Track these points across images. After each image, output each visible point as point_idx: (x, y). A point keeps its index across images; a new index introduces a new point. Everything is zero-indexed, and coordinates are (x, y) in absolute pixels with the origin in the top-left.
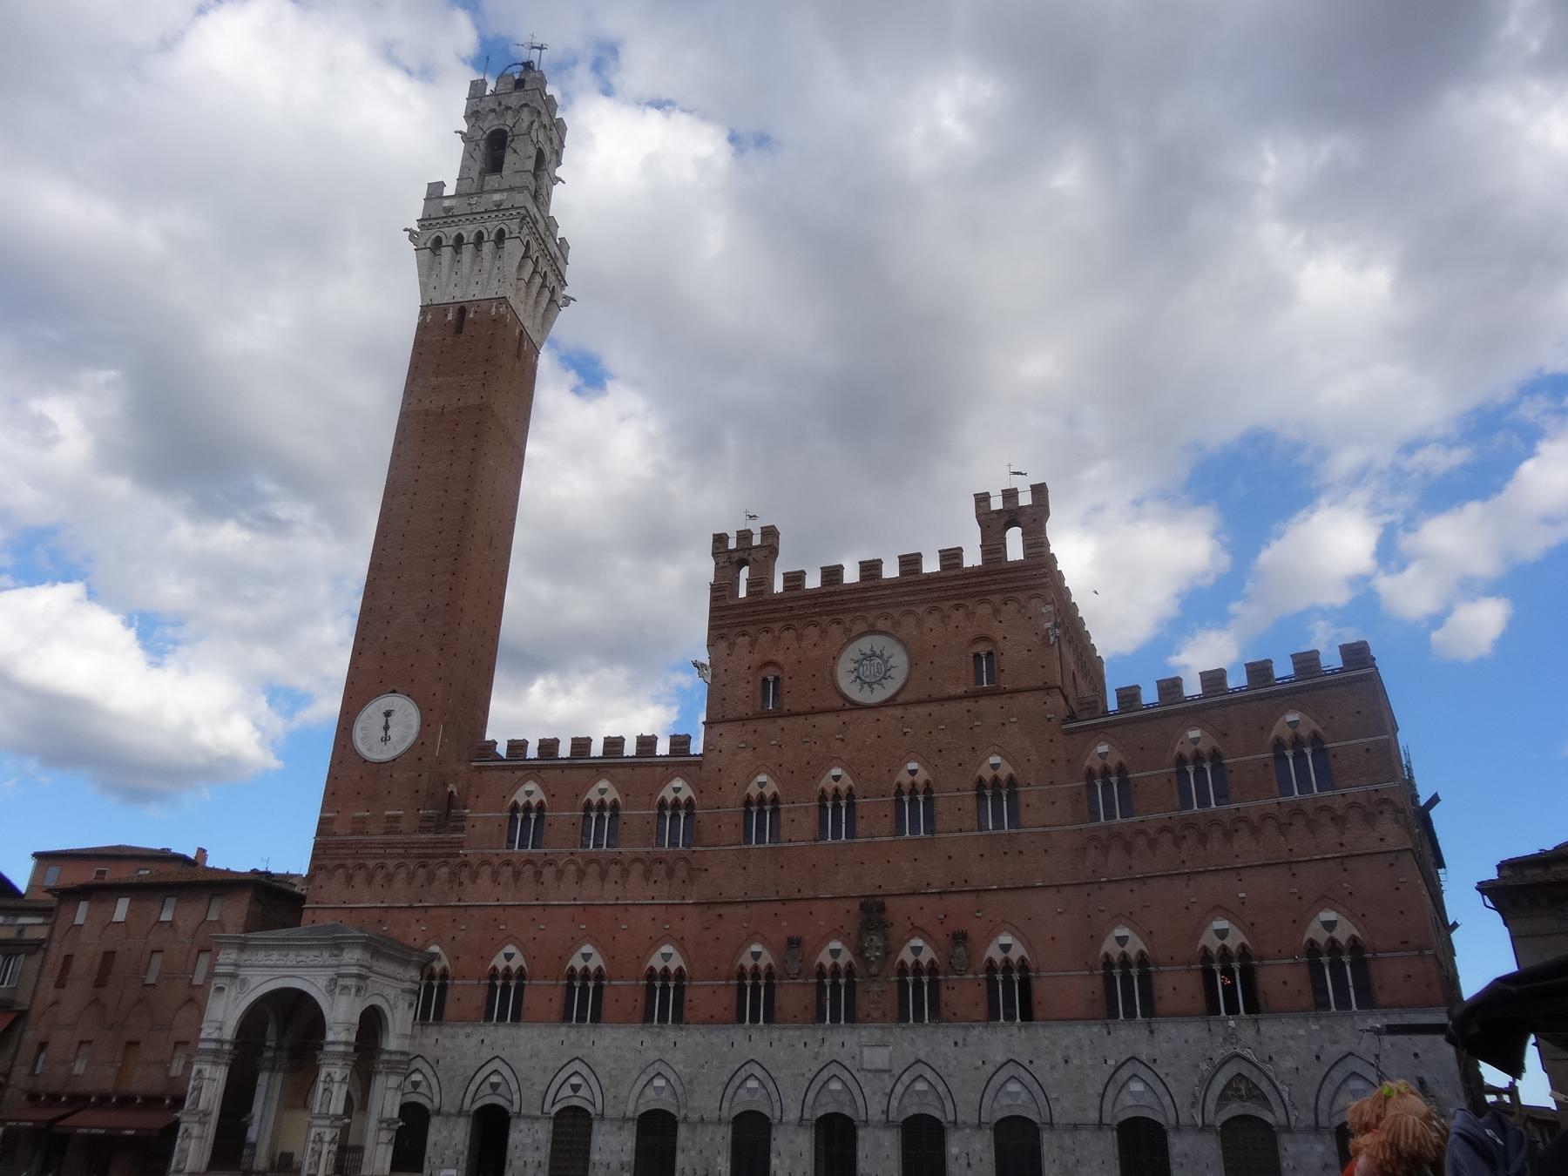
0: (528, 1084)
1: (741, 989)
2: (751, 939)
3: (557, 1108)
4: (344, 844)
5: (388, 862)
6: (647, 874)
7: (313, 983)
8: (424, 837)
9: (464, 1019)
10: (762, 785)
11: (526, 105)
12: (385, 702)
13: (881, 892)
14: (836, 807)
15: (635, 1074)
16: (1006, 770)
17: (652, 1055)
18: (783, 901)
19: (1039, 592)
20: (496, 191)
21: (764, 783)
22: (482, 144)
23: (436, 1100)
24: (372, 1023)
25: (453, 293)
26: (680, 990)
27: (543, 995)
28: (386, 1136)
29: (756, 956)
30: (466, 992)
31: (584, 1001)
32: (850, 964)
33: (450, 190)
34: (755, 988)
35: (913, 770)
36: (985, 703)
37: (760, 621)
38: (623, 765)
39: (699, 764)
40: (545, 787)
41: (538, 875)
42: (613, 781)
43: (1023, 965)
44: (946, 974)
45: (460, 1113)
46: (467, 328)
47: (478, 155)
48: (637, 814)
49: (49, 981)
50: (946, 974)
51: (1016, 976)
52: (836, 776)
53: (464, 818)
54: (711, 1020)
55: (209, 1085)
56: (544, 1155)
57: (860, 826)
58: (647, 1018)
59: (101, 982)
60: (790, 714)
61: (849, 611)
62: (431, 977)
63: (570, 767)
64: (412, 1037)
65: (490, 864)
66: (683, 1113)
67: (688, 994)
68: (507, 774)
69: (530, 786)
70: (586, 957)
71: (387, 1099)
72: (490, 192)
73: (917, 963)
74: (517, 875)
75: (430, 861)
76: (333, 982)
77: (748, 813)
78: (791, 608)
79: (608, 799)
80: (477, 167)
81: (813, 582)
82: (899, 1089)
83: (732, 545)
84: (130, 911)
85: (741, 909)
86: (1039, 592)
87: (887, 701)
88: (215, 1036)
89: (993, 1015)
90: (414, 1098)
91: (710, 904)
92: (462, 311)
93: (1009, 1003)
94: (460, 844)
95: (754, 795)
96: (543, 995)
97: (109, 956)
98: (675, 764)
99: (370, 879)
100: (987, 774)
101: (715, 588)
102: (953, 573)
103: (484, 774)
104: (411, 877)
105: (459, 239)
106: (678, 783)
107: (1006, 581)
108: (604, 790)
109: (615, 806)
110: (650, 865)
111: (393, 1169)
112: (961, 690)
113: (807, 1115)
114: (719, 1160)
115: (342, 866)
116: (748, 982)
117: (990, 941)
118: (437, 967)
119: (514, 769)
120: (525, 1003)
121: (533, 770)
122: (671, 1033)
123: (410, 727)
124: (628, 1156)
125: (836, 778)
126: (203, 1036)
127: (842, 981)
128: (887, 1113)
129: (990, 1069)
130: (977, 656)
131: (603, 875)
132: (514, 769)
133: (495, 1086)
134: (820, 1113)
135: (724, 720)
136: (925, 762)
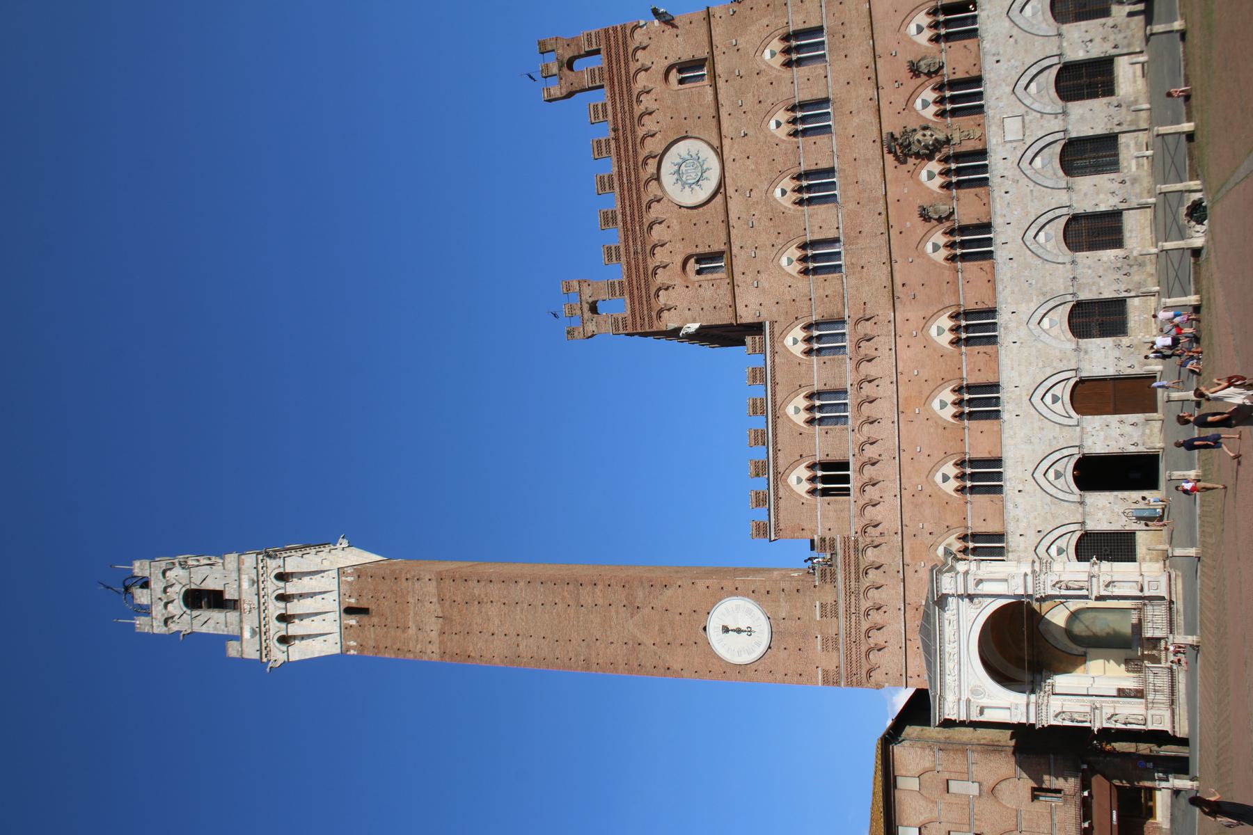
0: (1054, 442)
1: (964, 257)
2: (923, 254)
3: (1073, 413)
4: (848, 656)
5: (863, 609)
8: (840, 577)
9: (1002, 512)
10: (790, 261)
11: (164, 573)
12: (714, 634)
13: (878, 140)
14: (809, 188)
15: (1040, 345)
16: (777, 45)
17: (1023, 332)
18: (889, 227)
19: (628, 32)
20: (240, 586)
21: (789, 260)
22: (195, 613)
23: (1072, 527)
26: (968, 314)
28: (1105, 565)
29: (936, 248)
30: (979, 513)
31: (980, 401)
32: (940, 161)
34: (963, 244)
35: (777, 125)
36: (720, 69)
37: (646, 281)
38: (774, 395)
39: (772, 323)
40: (793, 466)
42: (787, 400)
43: (934, 12)
44: (943, 75)
45: (1082, 503)
46: (364, 604)
50: (943, 75)
51: (942, 18)
52: (782, 194)
53: (823, 540)
54: (992, 282)
56: (1113, 419)
57: (824, 165)
58: (992, 340)
60: (729, 242)
61: (639, 198)
62: (965, 551)
63: (775, 443)
64: (1019, 561)
65: (864, 508)
66: (1069, 298)
67: (971, 306)
68: (782, 503)
69: (792, 480)
70: (943, 405)
72: (240, 593)
73: (935, 102)
75: (862, 567)
77: (816, 271)
78: (636, 253)
82: (1036, 106)
85: (896, 267)
86: (628, 32)
87: (717, 153)
88: (1024, 710)
89: (973, 34)
90: (1072, 551)
92: (350, 611)
93: (963, 21)
94: (846, 540)
95: (799, 267)
98: (773, 346)
100: (781, 59)
102: (609, 108)
103: (782, 526)
107: (618, 61)
108: (795, 410)
109: (810, 397)
111: (1133, 560)
112: (710, 91)
113: (1064, 185)
114: (1105, 259)
115: (867, 655)
116: (959, 252)
117: (914, 43)
119: (777, 498)
120: (985, 455)
122: (1002, 318)
123: (738, 607)
124: (1108, 342)
125: (784, 192)
126: (1024, 721)
127: (953, 166)
128: (1056, 114)
129: (1015, 31)
130: (681, 81)
132: (777, 498)
133: (1058, 475)
134: (1061, 173)
135: (734, 306)
136: (769, 113)
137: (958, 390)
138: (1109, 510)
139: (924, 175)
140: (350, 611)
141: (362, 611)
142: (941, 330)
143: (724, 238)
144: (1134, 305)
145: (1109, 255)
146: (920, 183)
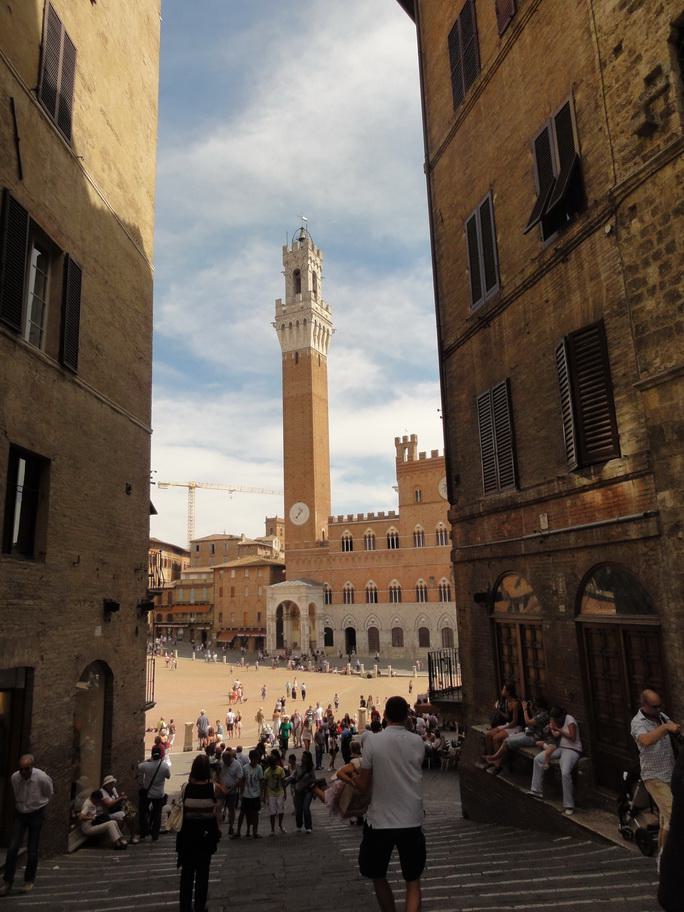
6: (387, 557)
7: (294, 599)
21: (419, 527)
24: (312, 608)
25: (292, 347)
26: (400, 592)
27: (360, 595)
28: (322, 637)
31: (373, 597)
33: (284, 302)
34: (422, 592)
41: (353, 559)
46: (299, 360)
47: (292, 281)
48: (381, 539)
49: (217, 595)
54: (409, 601)
55: (272, 627)
59: (232, 596)
67: (402, 594)
71: (320, 628)
74: (347, 559)
76: (299, 598)
79: (371, 534)
80: (292, 291)
81: (429, 456)
83: (401, 441)
84: (236, 573)
91: (405, 567)
92: (297, 354)
96: (360, 595)
97: (233, 589)
99: (303, 562)
101: (397, 459)
104: (315, 561)
105: (291, 324)
106: (392, 528)
108: (369, 531)
110: (387, 555)
118: (328, 588)
121: (347, 526)
131: (373, 558)
135: (404, 506)
137: (376, 589)
138: (340, 638)
139: (444, 578)
140: (297, 354)
141: (297, 362)
142: (395, 583)
143: (428, 501)
144: (402, 650)
145: (417, 643)
146: (442, 576)
